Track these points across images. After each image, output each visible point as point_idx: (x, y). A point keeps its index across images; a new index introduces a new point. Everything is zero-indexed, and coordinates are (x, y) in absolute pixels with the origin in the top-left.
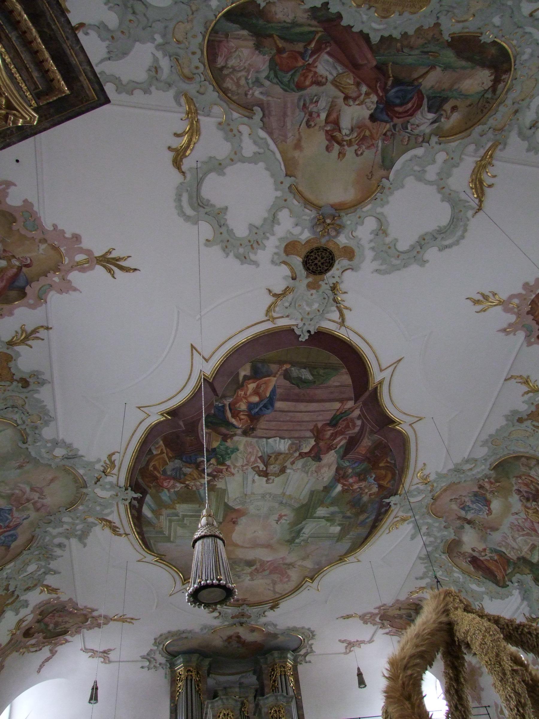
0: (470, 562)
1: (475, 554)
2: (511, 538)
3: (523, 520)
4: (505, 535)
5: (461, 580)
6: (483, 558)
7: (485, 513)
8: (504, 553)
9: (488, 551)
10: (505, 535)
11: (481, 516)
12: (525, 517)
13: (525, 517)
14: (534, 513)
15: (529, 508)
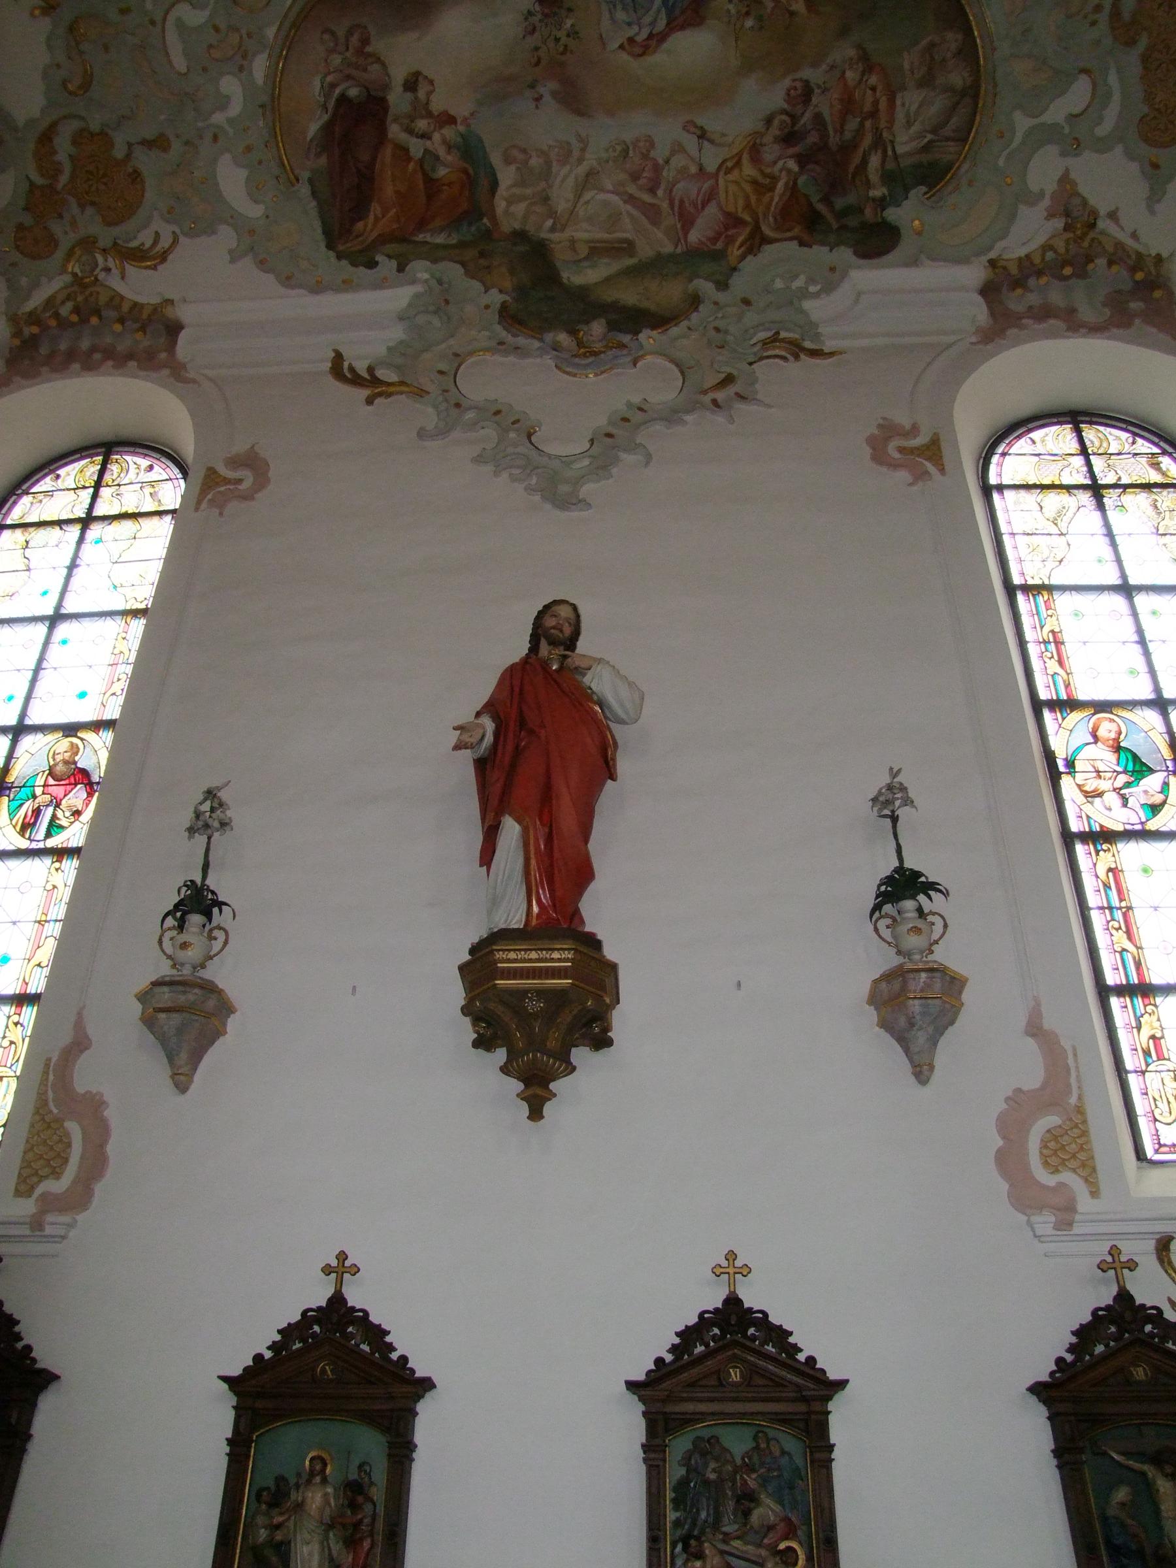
0: (343, 99)
1: (398, 100)
2: (582, 170)
3: (693, 169)
4: (576, 145)
5: (218, 118)
6: (403, 137)
7: (631, 33)
8: (494, 185)
9: (448, 132)
10: (576, 145)
11: (606, 23)
12: (711, 167)
13: (711, 167)
14: (754, 182)
15: (756, 159)
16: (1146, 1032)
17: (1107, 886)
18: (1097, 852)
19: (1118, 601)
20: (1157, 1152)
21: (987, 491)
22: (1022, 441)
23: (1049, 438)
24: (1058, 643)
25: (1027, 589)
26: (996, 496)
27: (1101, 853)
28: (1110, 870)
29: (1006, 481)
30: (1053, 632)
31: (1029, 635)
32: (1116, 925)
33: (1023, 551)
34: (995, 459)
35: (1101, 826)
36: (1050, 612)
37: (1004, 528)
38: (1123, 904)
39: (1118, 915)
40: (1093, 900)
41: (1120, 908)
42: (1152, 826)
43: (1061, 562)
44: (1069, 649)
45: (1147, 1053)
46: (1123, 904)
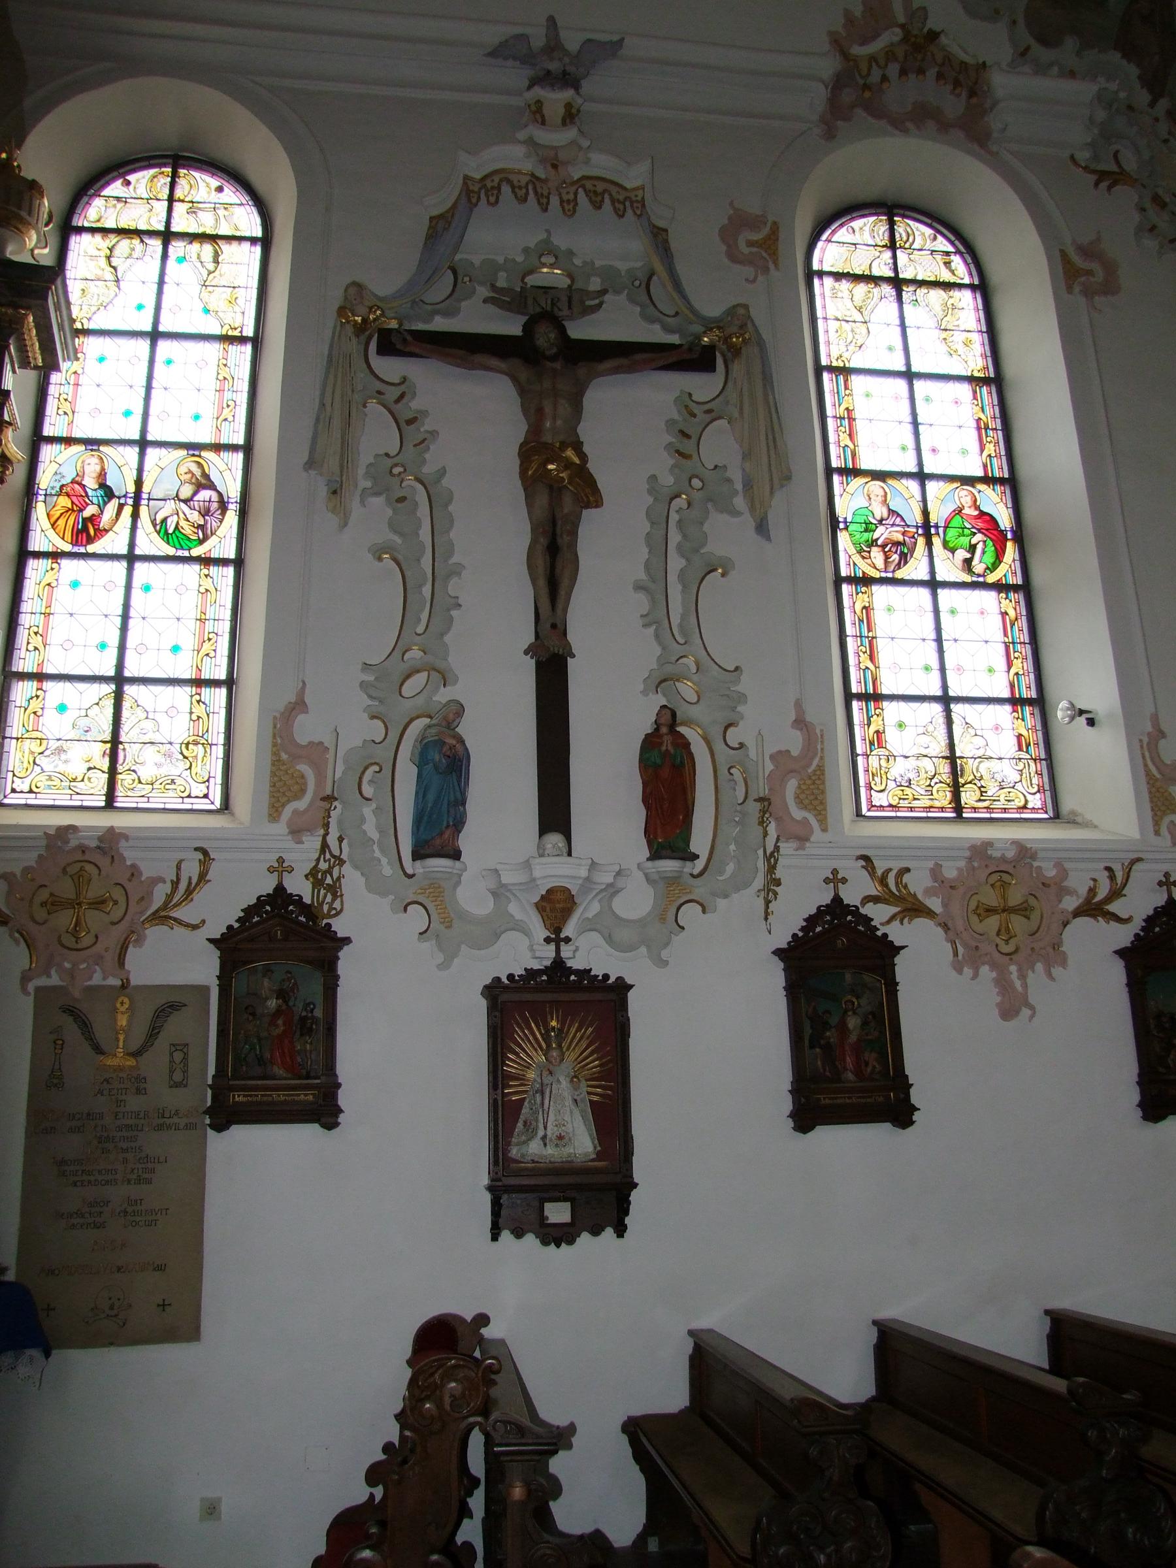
16: (873, 728)
17: (861, 621)
19: (901, 385)
21: (811, 275)
22: (844, 229)
23: (867, 228)
24: (851, 419)
25: (831, 369)
26: (816, 281)
28: (864, 607)
29: (826, 268)
30: (847, 409)
31: (830, 411)
33: (833, 336)
34: (820, 245)
36: (848, 392)
37: (820, 313)
38: (870, 634)
39: (866, 642)
40: (849, 630)
42: (899, 574)
44: (859, 425)
45: (872, 743)
46: (870, 634)
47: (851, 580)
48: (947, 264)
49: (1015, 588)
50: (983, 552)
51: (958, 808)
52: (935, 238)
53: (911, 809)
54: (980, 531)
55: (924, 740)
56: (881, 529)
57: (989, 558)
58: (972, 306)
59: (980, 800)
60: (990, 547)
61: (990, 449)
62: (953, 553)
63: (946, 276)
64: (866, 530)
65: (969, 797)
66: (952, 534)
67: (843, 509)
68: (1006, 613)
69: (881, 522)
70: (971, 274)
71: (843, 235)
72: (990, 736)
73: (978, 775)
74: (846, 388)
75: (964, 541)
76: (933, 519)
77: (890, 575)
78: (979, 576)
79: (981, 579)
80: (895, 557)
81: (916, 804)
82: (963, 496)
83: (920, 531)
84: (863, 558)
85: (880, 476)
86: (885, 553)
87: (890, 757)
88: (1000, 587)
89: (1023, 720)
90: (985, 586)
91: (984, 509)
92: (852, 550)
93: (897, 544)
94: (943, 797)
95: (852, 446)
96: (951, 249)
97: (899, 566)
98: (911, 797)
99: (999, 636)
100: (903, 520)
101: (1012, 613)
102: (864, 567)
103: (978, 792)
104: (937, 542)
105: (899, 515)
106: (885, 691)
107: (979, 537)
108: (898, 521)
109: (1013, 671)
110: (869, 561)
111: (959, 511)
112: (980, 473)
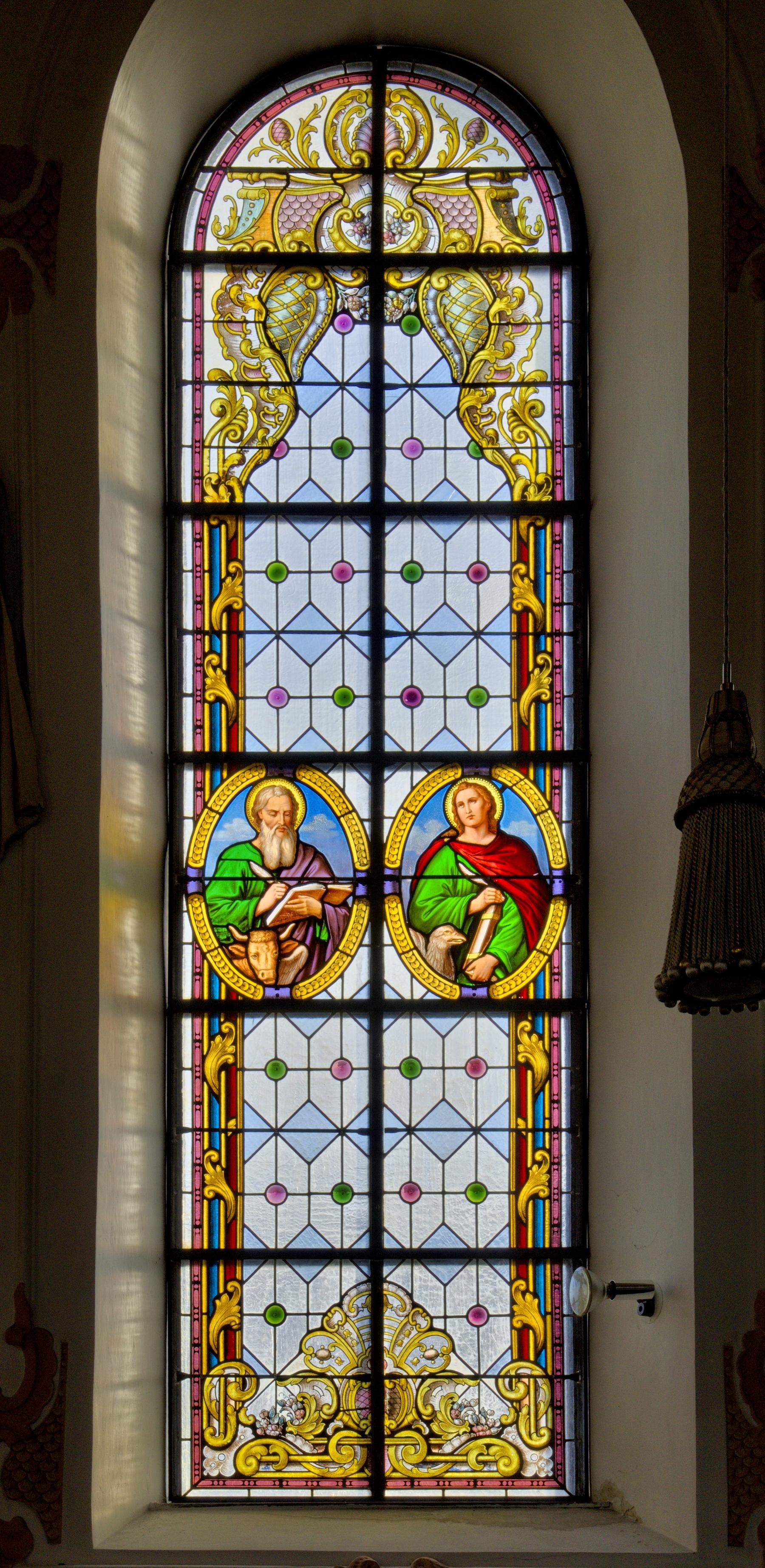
16: (217, 1322)
17: (214, 1096)
18: (212, 1038)
20: (194, 1486)
24: (236, 634)
25: (200, 511)
27: (218, 1039)
28: (225, 1067)
29: (212, 245)
30: (229, 610)
32: (215, 1158)
34: (203, 180)
35: (229, 989)
38: (232, 1123)
41: (226, 1131)
42: (304, 991)
43: (273, 449)
45: (212, 1352)
47: (197, 1008)
48: (502, 203)
49: (554, 1007)
50: (494, 929)
51: (377, 1480)
52: (479, 135)
53: (281, 1483)
54: (492, 882)
55: (319, 1341)
56: (276, 889)
57: (503, 946)
58: (546, 316)
59: (425, 1463)
60: (512, 920)
61: (539, 683)
62: (427, 936)
63: (494, 236)
64: (243, 896)
65: (400, 1457)
66: (428, 889)
67: (197, 845)
68: (528, 1065)
69: (277, 874)
70: (553, 228)
71: (259, 151)
72: (459, 1329)
73: (426, 1412)
74: (232, 556)
75: (455, 907)
76: (392, 858)
77: (284, 993)
78: (478, 984)
79: (481, 992)
80: (301, 951)
81: (292, 1472)
82: (466, 801)
83: (361, 890)
84: (232, 957)
85: (284, 765)
86: (279, 943)
87: (249, 1380)
88: (519, 1007)
89: (535, 1295)
90: (488, 1007)
91: (511, 829)
92: (209, 942)
93: (310, 921)
94: (347, 1460)
95: (228, 696)
96: (515, 161)
97: (306, 972)
98: (283, 1456)
99: (504, 1119)
100: (326, 865)
101: (540, 1063)
102: (232, 978)
103: (423, 1447)
104: (394, 911)
105: (317, 855)
106: (250, 1244)
107: (490, 894)
108: (316, 870)
109: (527, 1190)
110: (242, 964)
111: (450, 839)
112: (507, 745)
